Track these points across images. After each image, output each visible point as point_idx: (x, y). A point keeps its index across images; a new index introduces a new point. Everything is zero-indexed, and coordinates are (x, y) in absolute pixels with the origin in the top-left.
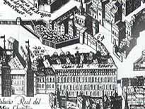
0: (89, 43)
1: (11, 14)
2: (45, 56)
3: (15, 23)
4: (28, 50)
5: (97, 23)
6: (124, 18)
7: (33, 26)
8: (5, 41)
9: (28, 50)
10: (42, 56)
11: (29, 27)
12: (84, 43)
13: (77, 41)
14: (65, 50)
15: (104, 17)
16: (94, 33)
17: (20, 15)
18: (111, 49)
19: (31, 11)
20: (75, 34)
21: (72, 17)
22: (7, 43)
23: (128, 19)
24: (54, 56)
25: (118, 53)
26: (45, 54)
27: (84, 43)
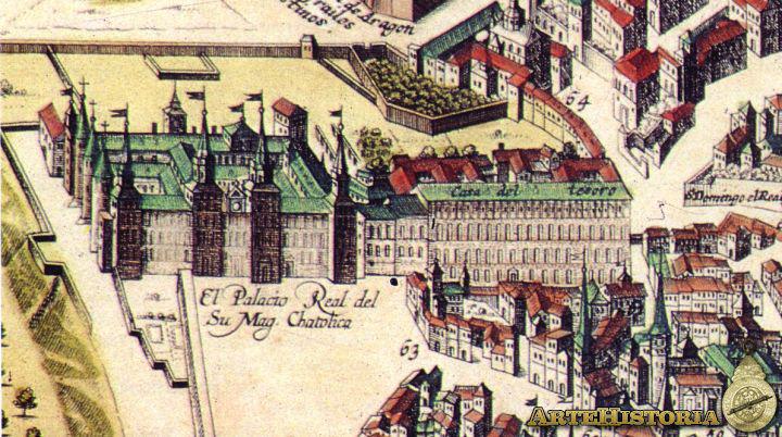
0: (539, 119)
1: (291, 30)
2: (395, 157)
3: (294, 52)
4: (340, 138)
5: (566, 56)
6: (654, 40)
7: (352, 62)
8: (262, 110)
9: (340, 138)
10: (385, 158)
11: (343, 65)
12: (520, 116)
13: (499, 111)
14: (461, 139)
15: (586, 35)
16: (556, 88)
17: (311, 28)
18: (611, 141)
19: (348, 15)
20: (492, 88)
21: (481, 36)
22: (269, 114)
23: (669, 42)
24: (423, 158)
25: (635, 151)
26: (394, 149)
27: (520, 116)
